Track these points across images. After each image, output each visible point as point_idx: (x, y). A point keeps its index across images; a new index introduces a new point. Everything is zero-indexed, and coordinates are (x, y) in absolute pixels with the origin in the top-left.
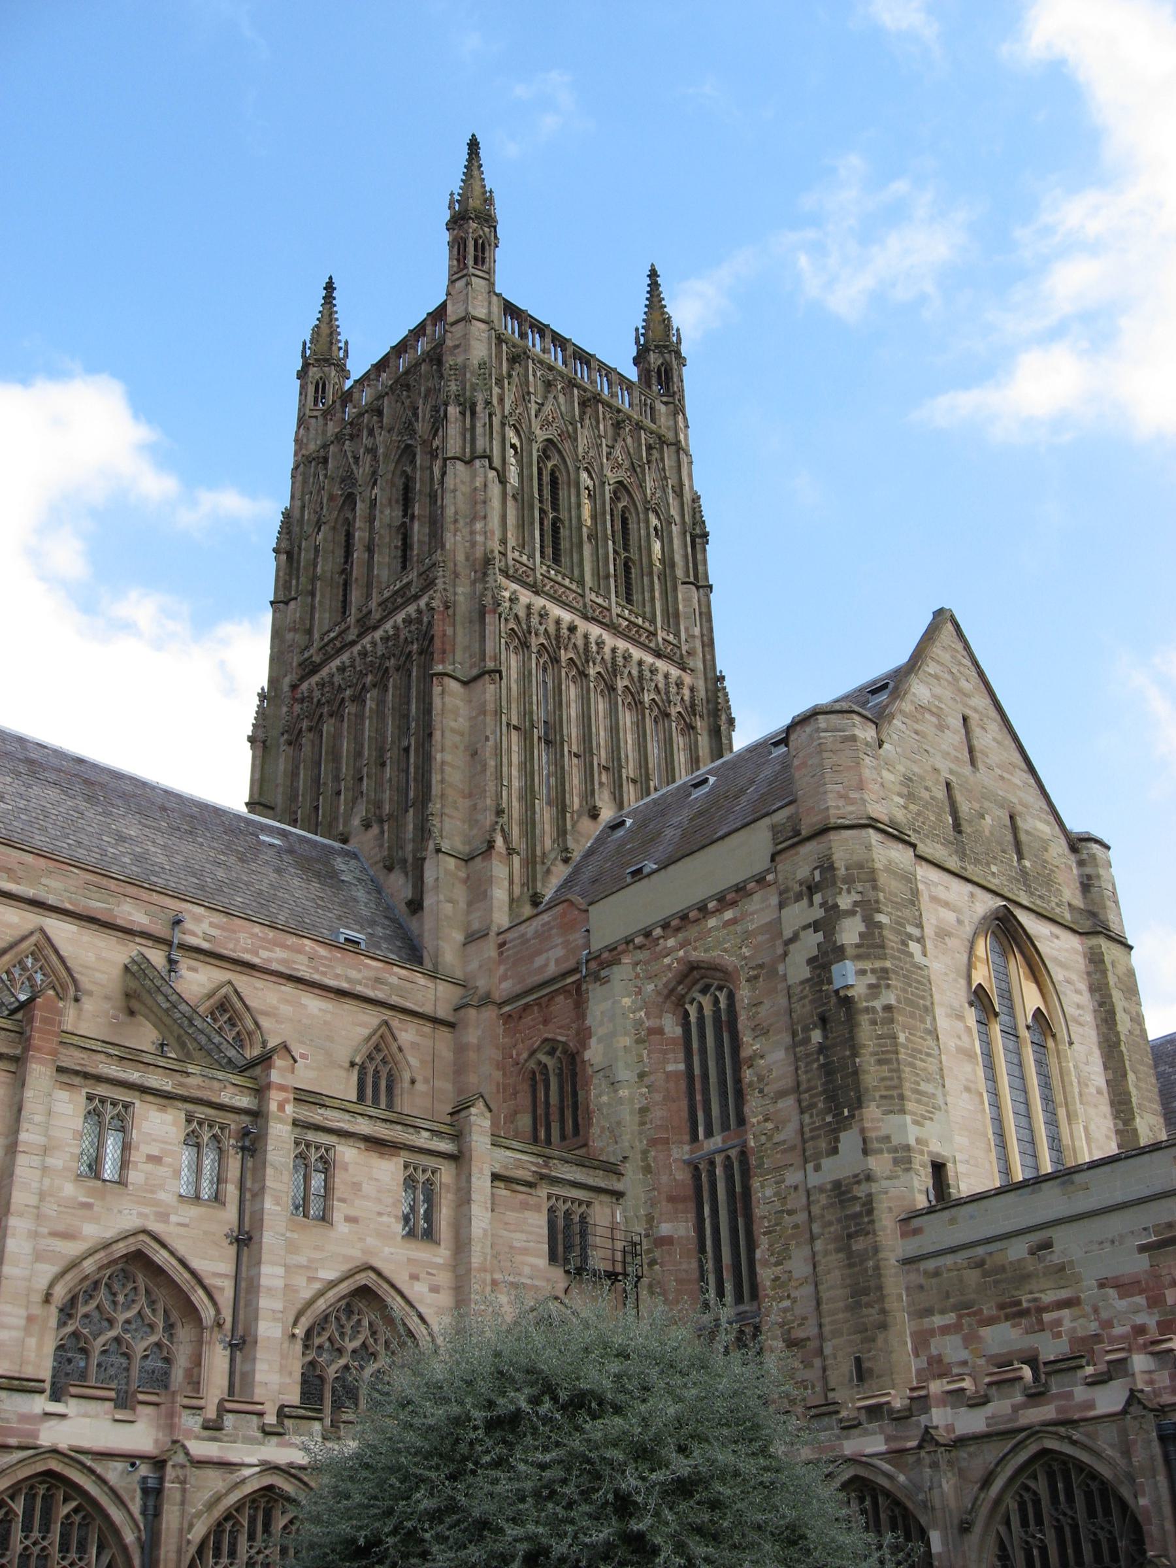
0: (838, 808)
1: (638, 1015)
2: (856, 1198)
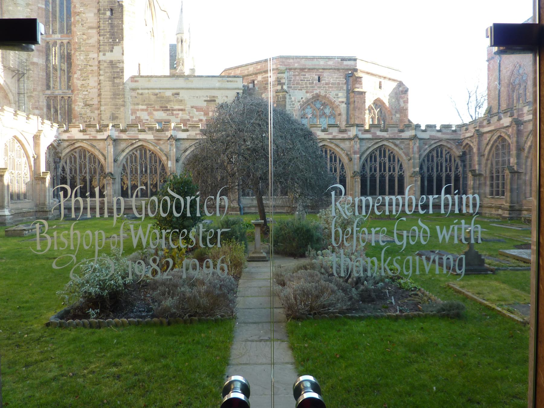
2: (118, 67)
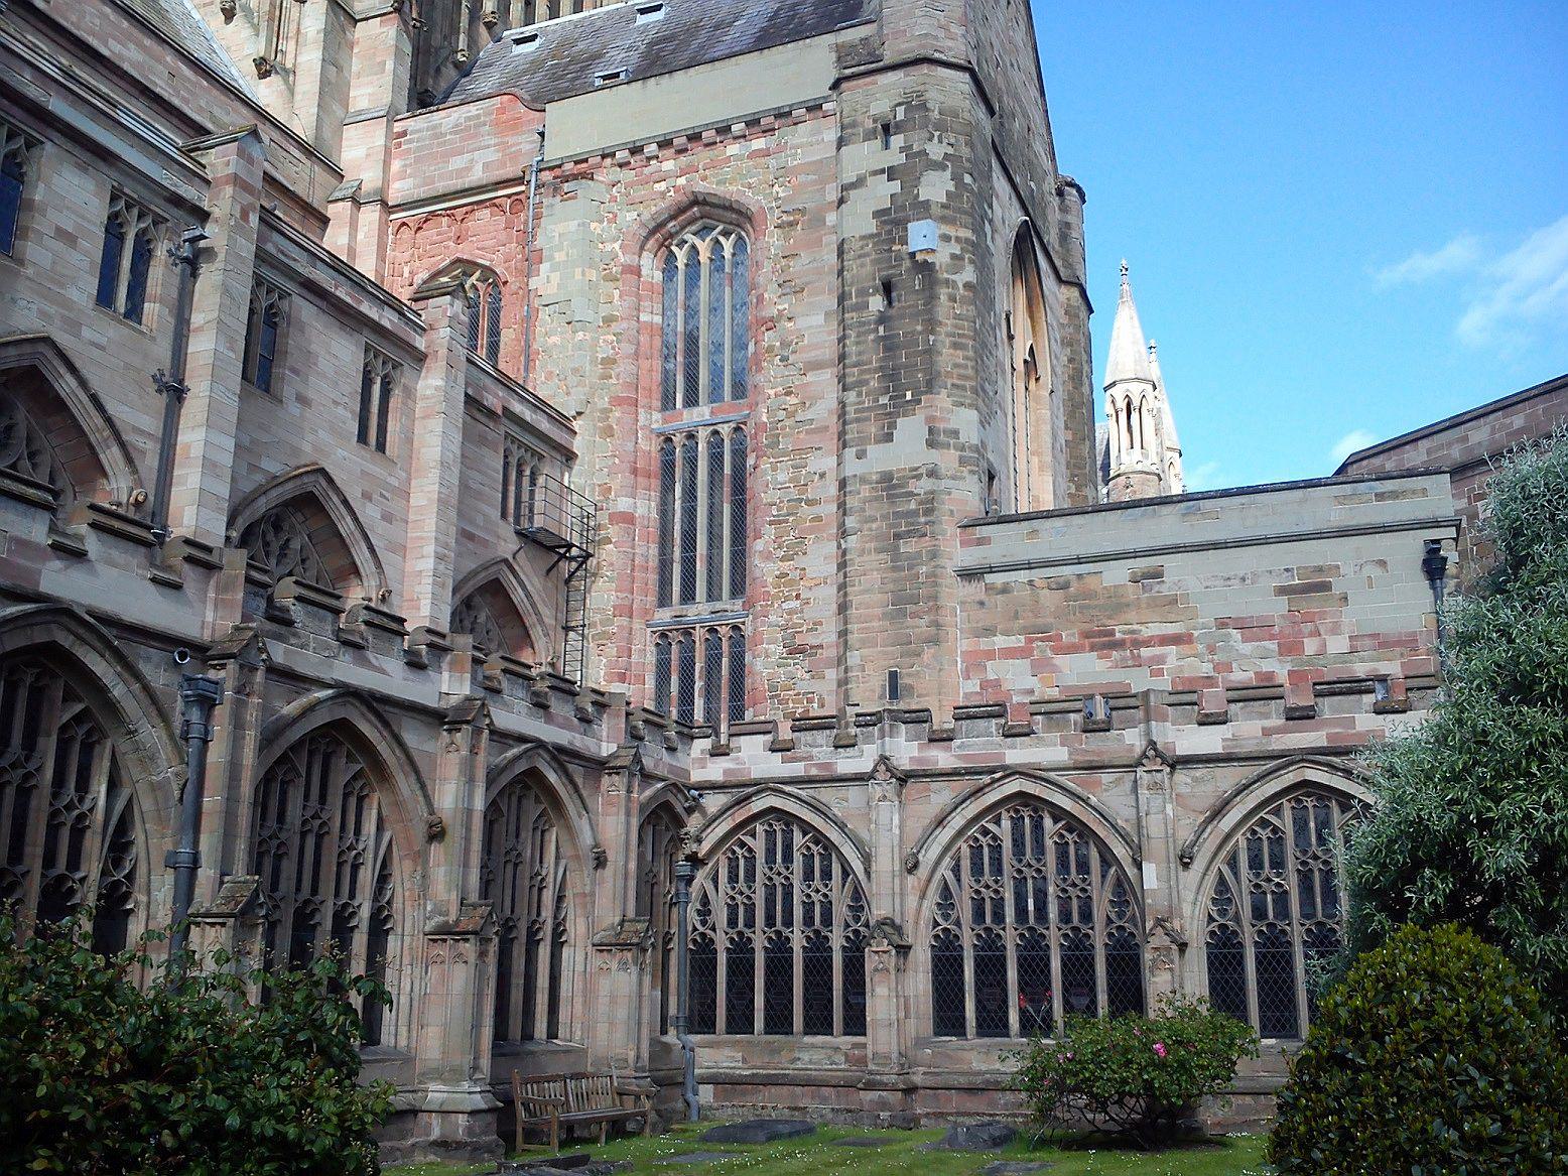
0: (936, 38)
1: (609, 247)
2: (911, 494)
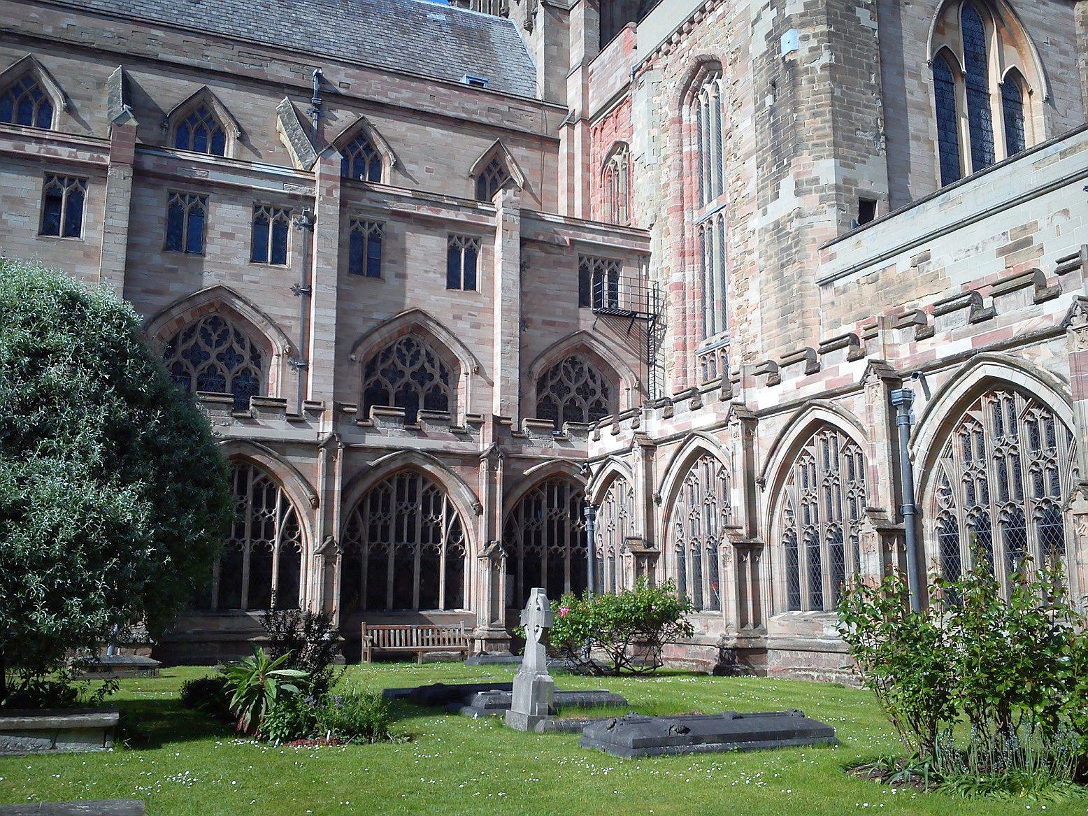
2: (789, 233)
